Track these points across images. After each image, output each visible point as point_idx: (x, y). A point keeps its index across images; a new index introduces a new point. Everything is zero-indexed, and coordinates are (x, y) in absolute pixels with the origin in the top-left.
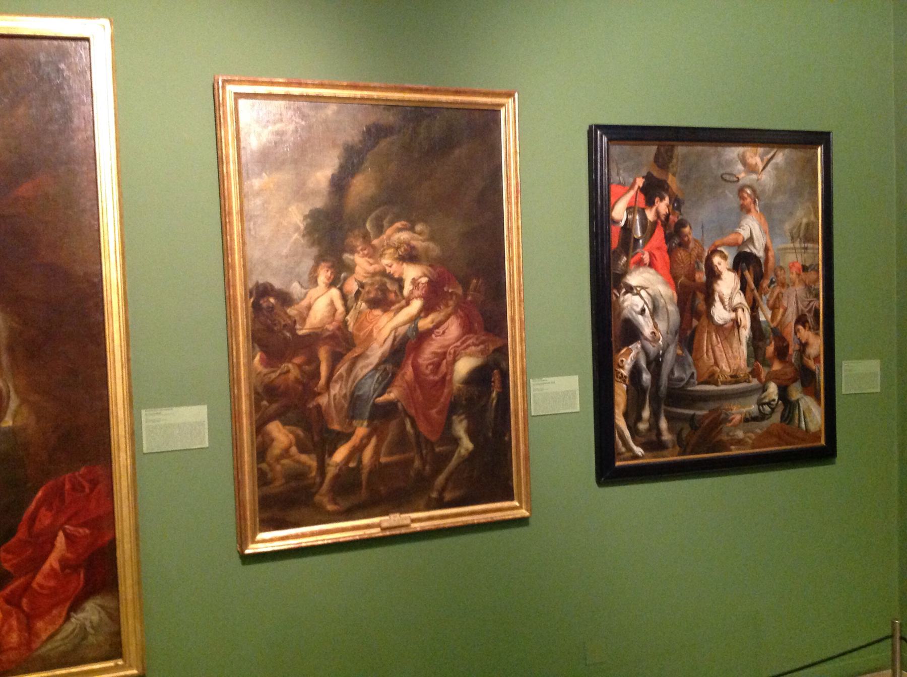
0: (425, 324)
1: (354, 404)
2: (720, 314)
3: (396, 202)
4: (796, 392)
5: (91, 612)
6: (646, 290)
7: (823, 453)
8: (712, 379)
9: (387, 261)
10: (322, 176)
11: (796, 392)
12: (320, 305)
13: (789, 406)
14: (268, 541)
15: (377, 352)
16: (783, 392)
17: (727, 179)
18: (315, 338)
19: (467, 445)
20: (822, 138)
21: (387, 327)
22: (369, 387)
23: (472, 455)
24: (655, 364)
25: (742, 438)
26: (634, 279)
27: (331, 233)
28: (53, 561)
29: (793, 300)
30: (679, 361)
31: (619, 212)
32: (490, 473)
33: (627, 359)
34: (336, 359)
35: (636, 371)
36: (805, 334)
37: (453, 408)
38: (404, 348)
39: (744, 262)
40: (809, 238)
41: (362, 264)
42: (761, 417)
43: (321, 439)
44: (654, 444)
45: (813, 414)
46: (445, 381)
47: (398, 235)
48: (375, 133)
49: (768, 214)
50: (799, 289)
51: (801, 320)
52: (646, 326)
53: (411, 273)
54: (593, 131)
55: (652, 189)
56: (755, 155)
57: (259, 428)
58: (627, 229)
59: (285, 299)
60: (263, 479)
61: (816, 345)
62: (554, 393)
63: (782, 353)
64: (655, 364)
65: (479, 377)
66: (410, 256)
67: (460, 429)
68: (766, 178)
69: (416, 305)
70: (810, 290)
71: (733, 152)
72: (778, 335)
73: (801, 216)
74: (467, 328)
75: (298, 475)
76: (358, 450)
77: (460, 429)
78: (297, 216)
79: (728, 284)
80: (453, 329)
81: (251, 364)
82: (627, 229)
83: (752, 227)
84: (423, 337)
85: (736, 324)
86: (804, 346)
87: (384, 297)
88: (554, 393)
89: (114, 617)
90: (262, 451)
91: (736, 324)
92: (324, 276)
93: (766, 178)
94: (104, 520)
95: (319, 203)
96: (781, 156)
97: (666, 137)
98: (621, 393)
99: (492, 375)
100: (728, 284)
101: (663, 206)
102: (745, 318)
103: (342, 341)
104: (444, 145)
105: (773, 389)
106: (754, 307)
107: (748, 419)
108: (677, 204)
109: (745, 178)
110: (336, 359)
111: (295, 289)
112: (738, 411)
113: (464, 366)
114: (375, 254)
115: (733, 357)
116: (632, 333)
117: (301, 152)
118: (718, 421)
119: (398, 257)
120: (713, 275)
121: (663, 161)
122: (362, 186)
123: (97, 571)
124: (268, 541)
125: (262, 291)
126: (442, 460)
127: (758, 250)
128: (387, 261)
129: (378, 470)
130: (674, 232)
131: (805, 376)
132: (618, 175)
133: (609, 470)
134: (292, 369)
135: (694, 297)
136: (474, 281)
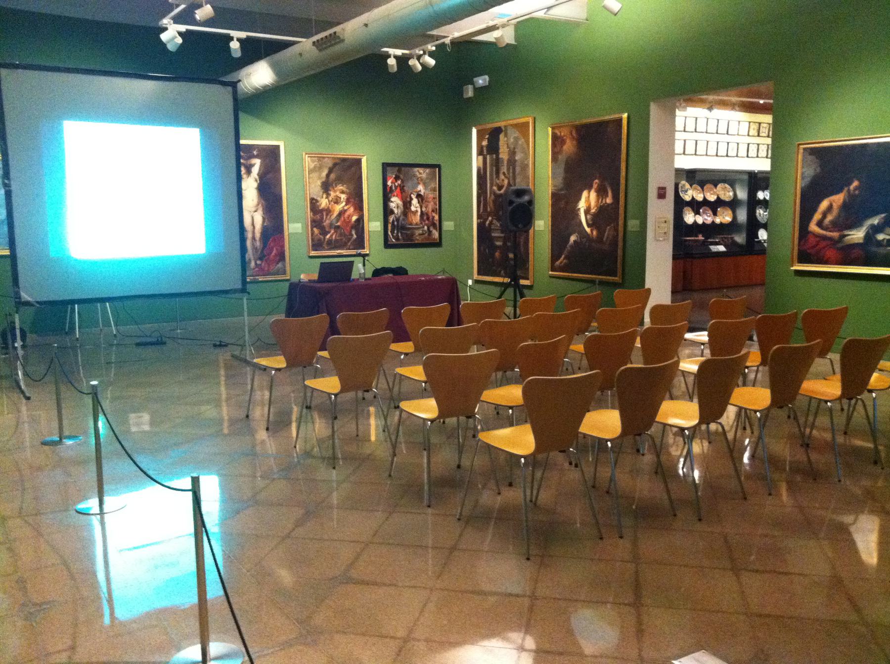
0: (346, 208)
1: (331, 225)
2: (413, 208)
3: (339, 180)
4: (431, 229)
5: (280, 265)
6: (396, 202)
7: (438, 244)
8: (411, 224)
9: (338, 193)
10: (324, 174)
11: (431, 229)
12: (324, 203)
13: (430, 232)
14: (313, 253)
15: (336, 214)
16: (428, 229)
17: (414, 176)
18: (323, 210)
19: (355, 236)
20: (439, 166)
21: (338, 208)
22: (334, 221)
23: (355, 240)
24: (398, 220)
25: (418, 239)
26: (392, 199)
27: (326, 187)
28: (273, 254)
29: (431, 206)
30: (403, 220)
31: (389, 183)
32: (360, 243)
33: (391, 218)
34: (327, 215)
35: (393, 221)
36: (434, 214)
37: (352, 228)
38: (342, 213)
39: (419, 196)
40: (434, 190)
41: (332, 193)
42: (423, 234)
43: (325, 233)
44: (397, 239)
45: (436, 234)
46: (350, 221)
47: (340, 187)
48: (335, 165)
49: (424, 184)
50: (432, 203)
51: (433, 211)
52: (396, 211)
53: (343, 196)
54: (383, 164)
55: (397, 178)
56: (421, 170)
57: (312, 230)
58: (391, 187)
59: (317, 201)
60: (313, 240)
61: (437, 217)
62: (374, 226)
63: (428, 219)
64: (398, 220)
65: (358, 221)
66: (343, 192)
67: (353, 232)
68: (424, 176)
69: (344, 204)
70: (435, 204)
71: (416, 169)
72: (427, 214)
73: (433, 185)
74: (355, 209)
75: (319, 240)
76: (332, 236)
77: (353, 232)
78: (319, 183)
79: (415, 201)
80: (352, 209)
81: (309, 214)
82: (391, 187)
83: (421, 188)
84: (345, 211)
85: (417, 211)
86: (433, 217)
87: (337, 201)
88: (374, 226)
89: (285, 266)
90: (312, 234)
91: (417, 211)
92: (325, 196)
93: (424, 176)
94: (283, 246)
95: (324, 180)
96: (428, 170)
97: (400, 166)
98: (390, 226)
99: (360, 220)
100: (415, 201)
101: (399, 182)
102: (419, 210)
103: (328, 211)
104: (350, 167)
105: (426, 228)
106: (421, 207)
107: (420, 235)
108: (403, 182)
109: (419, 176)
110: (327, 215)
111: (319, 199)
112: (417, 232)
113: (354, 218)
114: (335, 191)
115: (416, 219)
116: (392, 212)
117: (319, 168)
118: (413, 235)
119: (340, 192)
120: (411, 199)
121: (399, 171)
122: (332, 176)
123: (281, 257)
124: (313, 253)
125: (312, 199)
126: (350, 239)
127: (422, 193)
128: (338, 193)
129: (336, 240)
130: (402, 188)
131: (434, 225)
132: (389, 175)
133: (387, 245)
134: (318, 217)
135: (407, 204)
136: (356, 198)
